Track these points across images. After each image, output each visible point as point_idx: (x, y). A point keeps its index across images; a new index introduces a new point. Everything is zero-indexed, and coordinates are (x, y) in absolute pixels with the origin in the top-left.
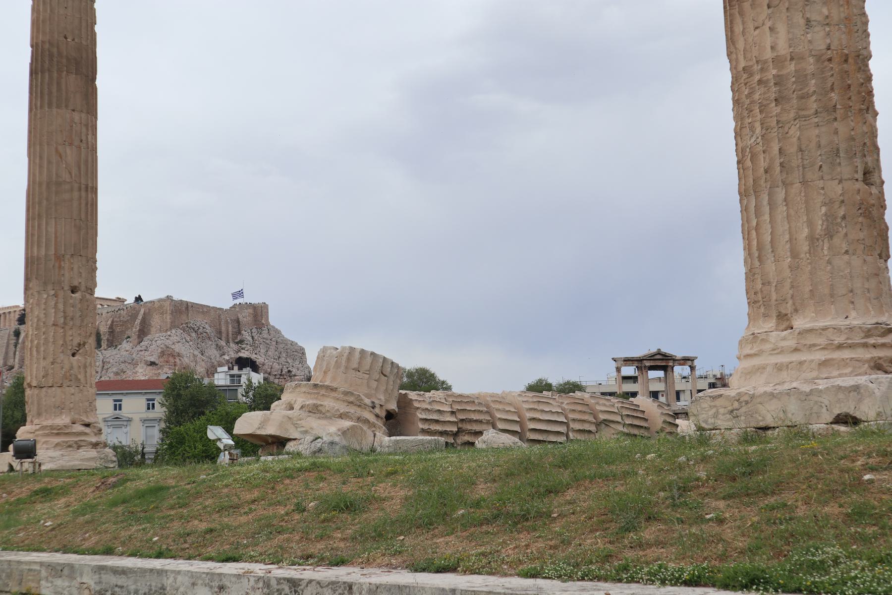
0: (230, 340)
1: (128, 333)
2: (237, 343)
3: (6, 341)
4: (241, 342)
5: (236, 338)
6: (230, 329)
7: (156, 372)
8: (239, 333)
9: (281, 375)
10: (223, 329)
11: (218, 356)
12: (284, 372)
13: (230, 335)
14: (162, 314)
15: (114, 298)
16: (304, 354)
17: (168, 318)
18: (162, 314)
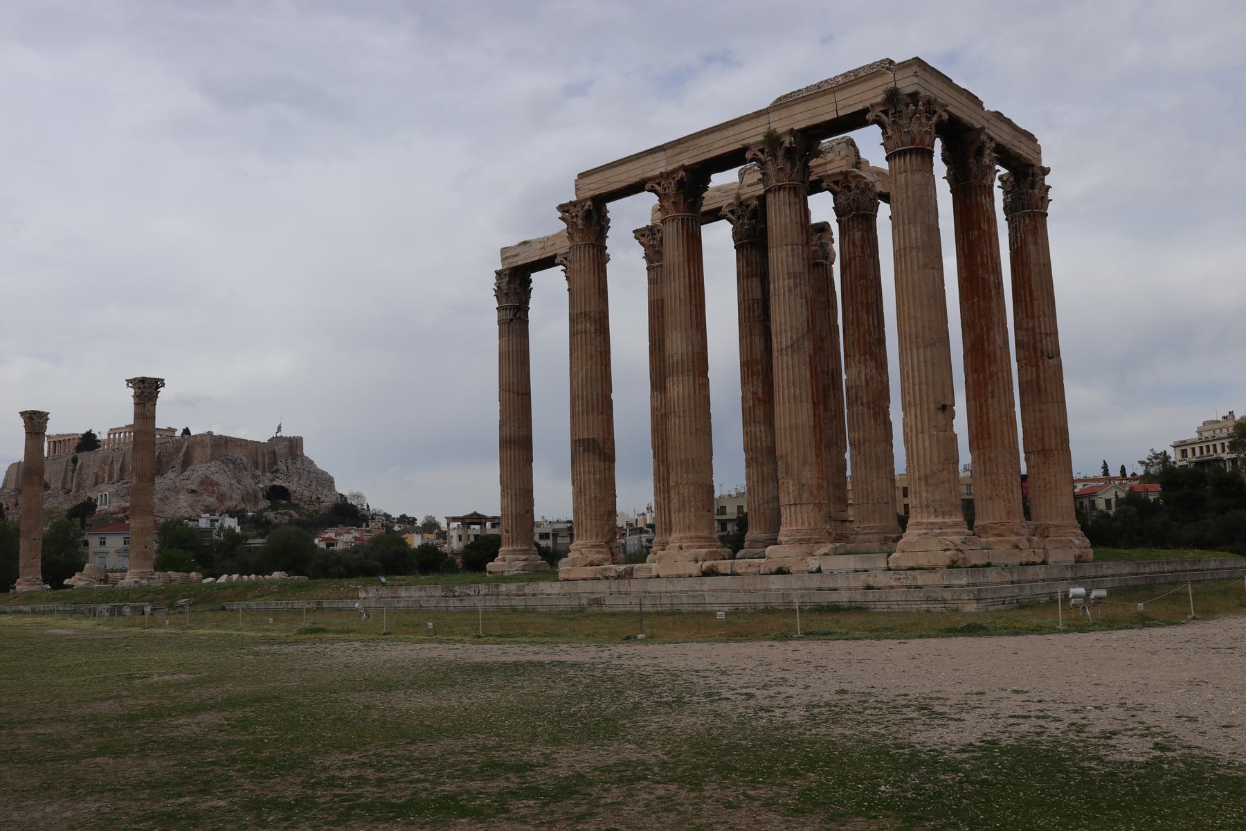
0: (267, 470)
1: (173, 463)
2: (273, 472)
3: (64, 467)
4: (277, 471)
5: (272, 468)
6: (266, 460)
7: (197, 499)
8: (275, 463)
9: (310, 501)
10: (260, 459)
11: (253, 484)
12: (313, 499)
13: (267, 465)
14: (203, 447)
15: (166, 428)
16: (332, 482)
17: (209, 451)
18: (203, 447)
